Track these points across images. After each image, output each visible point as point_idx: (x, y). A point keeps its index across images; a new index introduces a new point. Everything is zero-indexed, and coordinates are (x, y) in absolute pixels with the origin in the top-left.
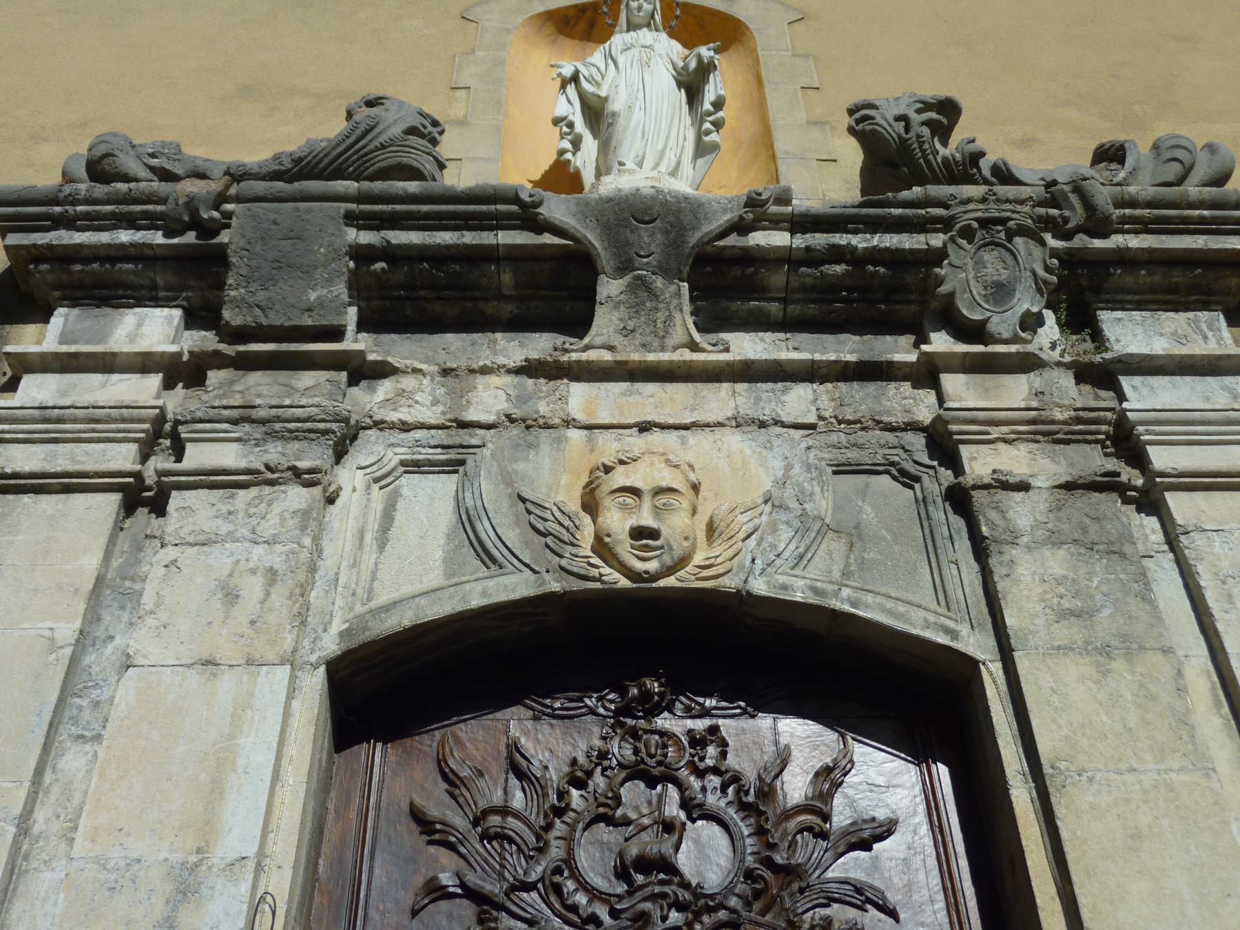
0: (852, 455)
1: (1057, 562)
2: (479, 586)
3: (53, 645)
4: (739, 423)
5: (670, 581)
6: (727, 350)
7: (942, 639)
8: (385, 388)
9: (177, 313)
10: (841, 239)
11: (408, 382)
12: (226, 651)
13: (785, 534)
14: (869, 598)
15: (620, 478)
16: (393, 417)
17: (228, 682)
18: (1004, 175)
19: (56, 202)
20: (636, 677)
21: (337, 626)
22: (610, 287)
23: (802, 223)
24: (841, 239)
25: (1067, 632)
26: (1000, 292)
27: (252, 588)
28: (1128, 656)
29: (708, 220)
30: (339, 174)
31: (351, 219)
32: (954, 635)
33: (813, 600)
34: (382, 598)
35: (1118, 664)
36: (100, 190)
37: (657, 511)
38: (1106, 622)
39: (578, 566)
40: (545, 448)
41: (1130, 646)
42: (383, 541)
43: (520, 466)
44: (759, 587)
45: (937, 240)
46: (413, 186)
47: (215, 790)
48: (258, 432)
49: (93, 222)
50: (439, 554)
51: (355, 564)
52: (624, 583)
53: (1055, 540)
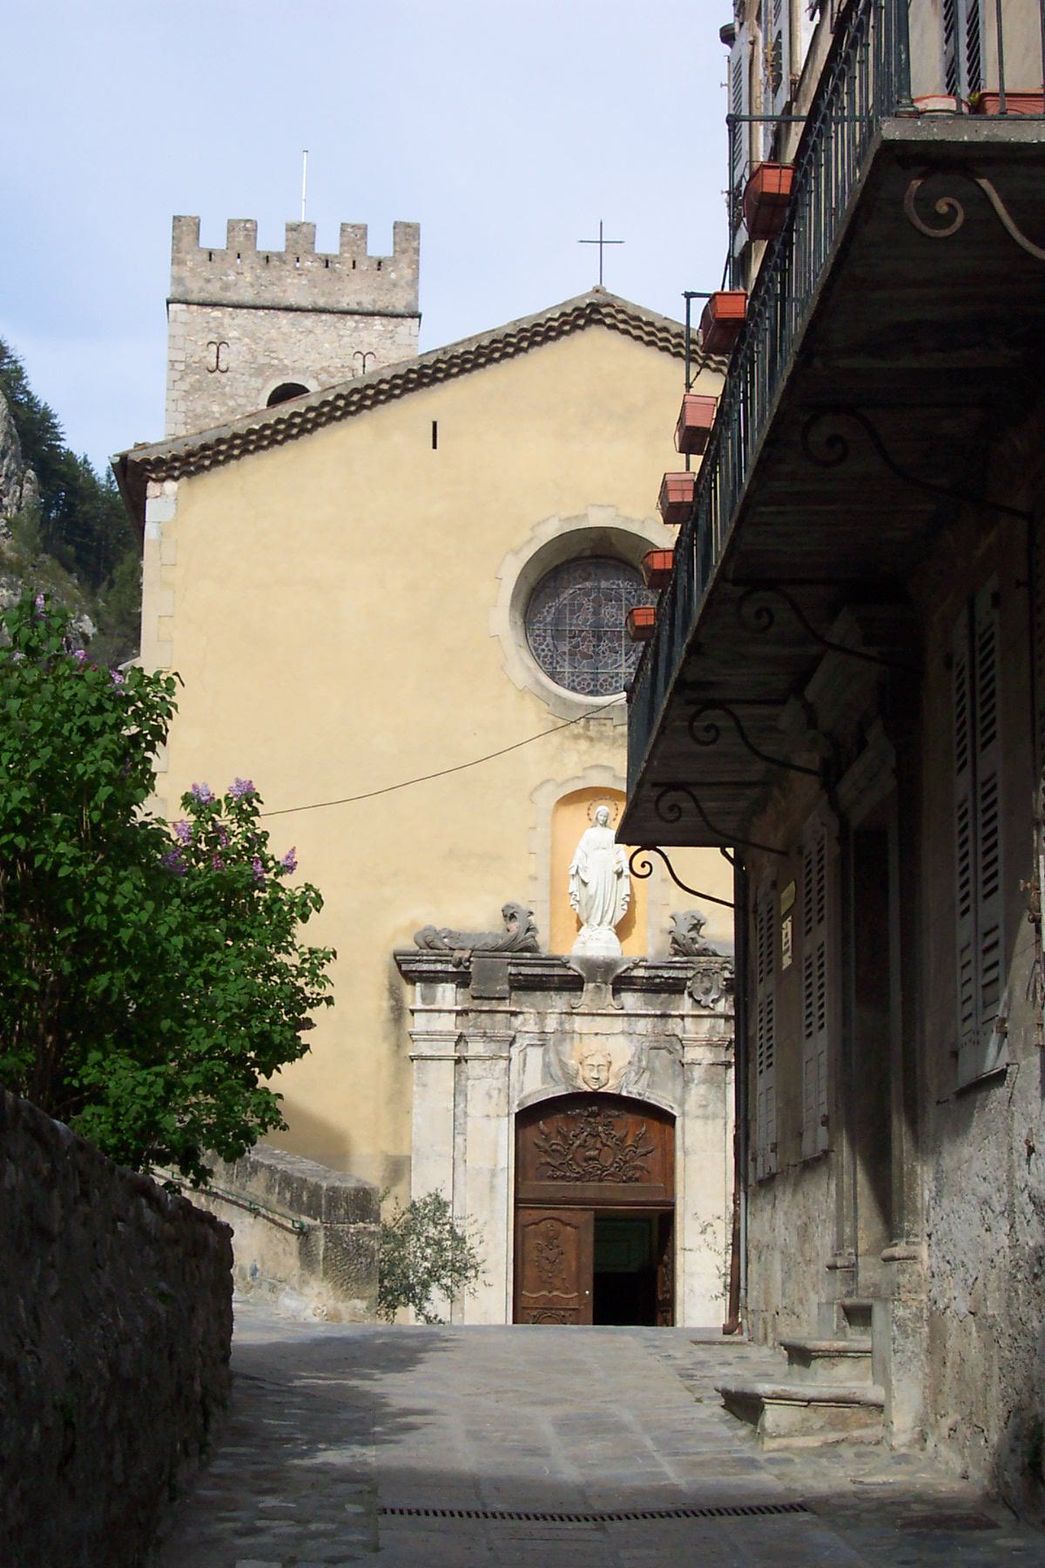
0: (655, 1045)
1: (702, 1089)
2: (551, 1090)
3: (448, 1111)
4: (623, 1033)
5: (601, 1090)
6: (622, 1009)
7: (669, 1110)
8: (521, 1017)
9: (454, 986)
10: (660, 972)
11: (527, 1016)
12: (492, 1114)
13: (633, 1074)
14: (653, 1096)
15: (589, 1061)
16: (524, 1029)
17: (494, 1122)
18: (716, 955)
19: (416, 955)
20: (591, 1106)
21: (517, 1102)
22: (589, 986)
23: (647, 968)
24: (660, 972)
25: (700, 1112)
26: (707, 992)
27: (495, 1093)
28: (713, 1119)
29: (621, 966)
30: (505, 951)
31: (509, 964)
32: (672, 1108)
33: (638, 1097)
34: (525, 1093)
35: (710, 1122)
36: (431, 952)
37: (598, 1071)
38: (710, 1109)
39: (578, 1085)
40: (568, 1041)
41: (715, 1116)
42: (524, 1071)
43: (560, 1048)
44: (624, 1094)
45: (690, 974)
46: (528, 955)
47: (496, 1151)
48: (488, 1040)
49: (428, 962)
50: (539, 1076)
51: (519, 1081)
52: (590, 1090)
53: (704, 1082)
